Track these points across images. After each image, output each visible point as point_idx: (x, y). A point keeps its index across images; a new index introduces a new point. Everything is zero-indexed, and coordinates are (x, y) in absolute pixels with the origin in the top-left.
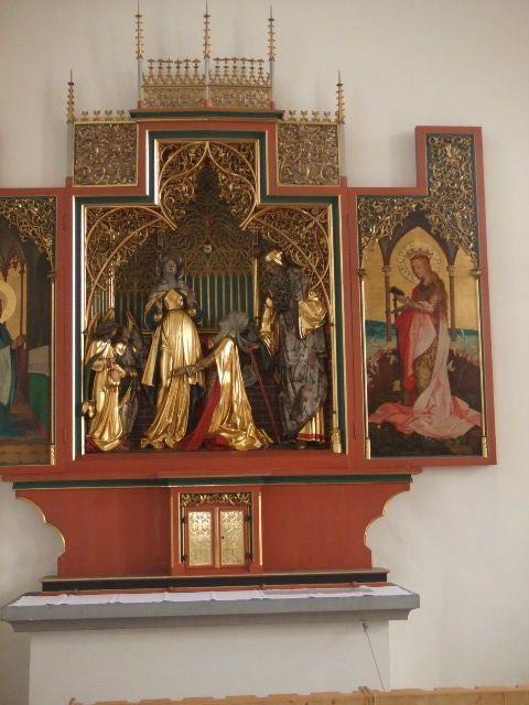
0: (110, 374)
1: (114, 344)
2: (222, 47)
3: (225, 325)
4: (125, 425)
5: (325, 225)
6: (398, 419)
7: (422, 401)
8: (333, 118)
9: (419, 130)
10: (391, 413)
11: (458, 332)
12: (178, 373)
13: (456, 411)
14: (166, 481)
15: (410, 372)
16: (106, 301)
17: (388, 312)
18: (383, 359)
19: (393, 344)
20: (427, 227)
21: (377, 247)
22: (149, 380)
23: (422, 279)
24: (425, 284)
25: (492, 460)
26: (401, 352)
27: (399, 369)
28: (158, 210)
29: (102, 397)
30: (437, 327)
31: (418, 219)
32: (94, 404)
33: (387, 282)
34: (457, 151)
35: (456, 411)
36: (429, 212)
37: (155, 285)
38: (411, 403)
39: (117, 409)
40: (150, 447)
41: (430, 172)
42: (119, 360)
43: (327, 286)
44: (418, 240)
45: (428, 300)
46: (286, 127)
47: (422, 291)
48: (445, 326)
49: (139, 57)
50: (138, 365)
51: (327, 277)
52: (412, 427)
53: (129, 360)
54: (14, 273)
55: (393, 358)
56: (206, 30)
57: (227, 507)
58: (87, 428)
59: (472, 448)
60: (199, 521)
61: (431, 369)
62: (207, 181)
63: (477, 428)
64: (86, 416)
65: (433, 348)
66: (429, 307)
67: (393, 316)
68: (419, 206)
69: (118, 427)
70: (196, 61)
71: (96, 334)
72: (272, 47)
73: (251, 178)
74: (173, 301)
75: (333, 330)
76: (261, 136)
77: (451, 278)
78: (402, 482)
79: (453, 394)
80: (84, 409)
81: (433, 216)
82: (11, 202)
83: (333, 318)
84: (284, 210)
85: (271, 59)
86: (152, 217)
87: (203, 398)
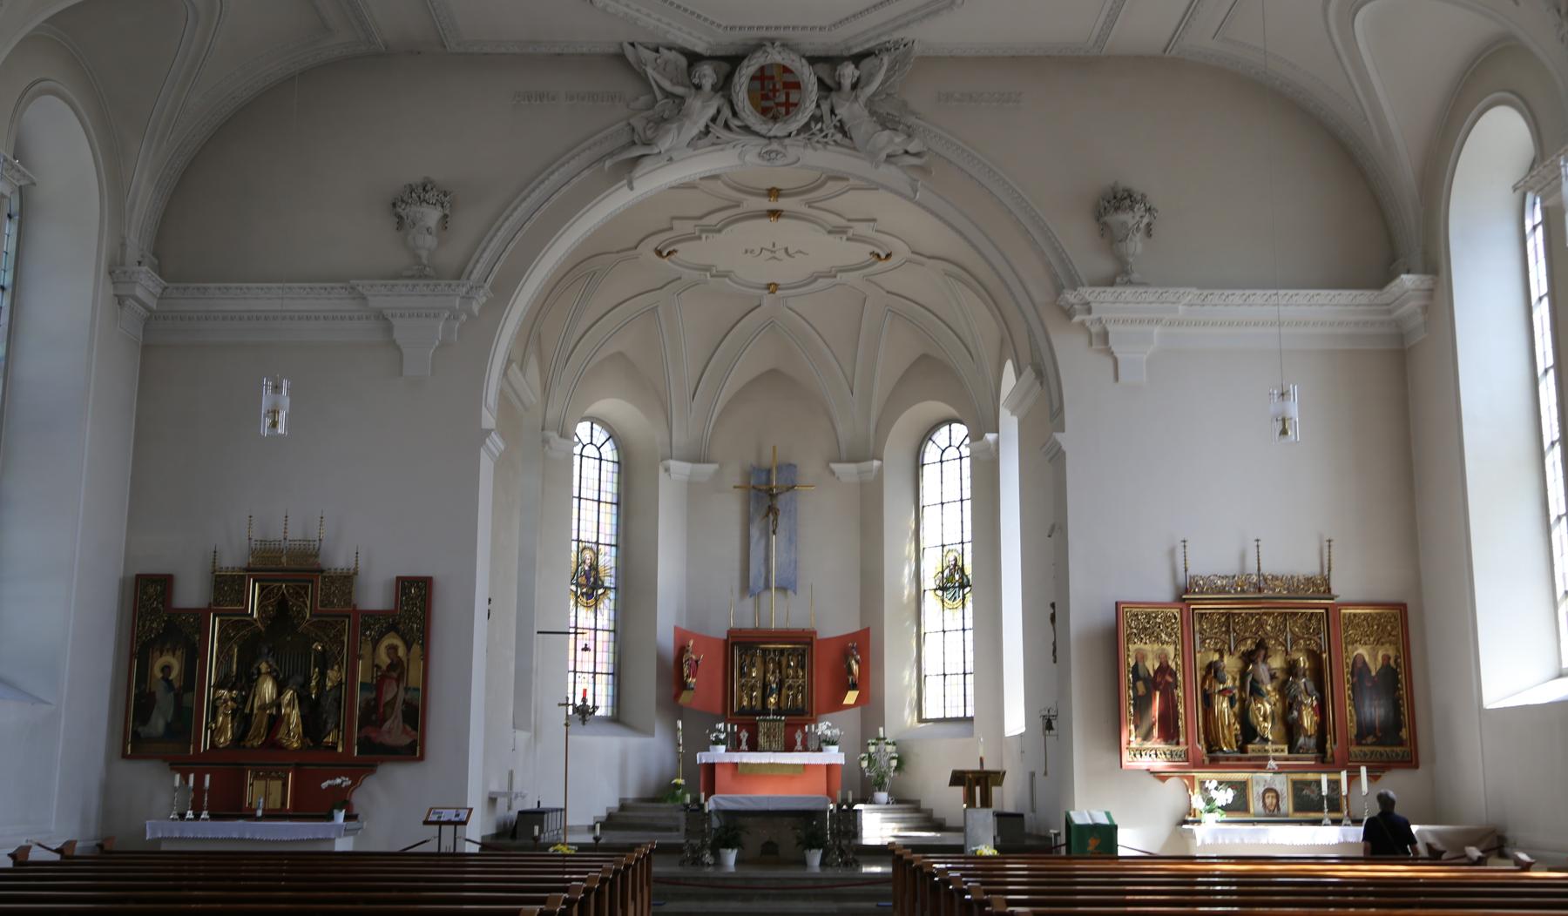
0: (225, 708)
1: (230, 690)
2: (296, 534)
4: (233, 734)
6: (373, 735)
7: (387, 725)
8: (352, 571)
11: (409, 689)
12: (263, 707)
14: (243, 764)
15: (382, 710)
16: (231, 667)
17: (372, 678)
19: (373, 695)
20: (397, 631)
21: (370, 643)
22: (247, 711)
23: (392, 660)
24: (395, 662)
25: (422, 758)
28: (255, 620)
30: (398, 687)
31: (393, 628)
32: (216, 723)
33: (373, 661)
35: (405, 731)
36: (398, 623)
38: (381, 726)
39: (230, 726)
40: (244, 746)
42: (233, 699)
43: (343, 663)
44: (392, 639)
45: (394, 671)
46: (325, 577)
47: (391, 667)
49: (250, 539)
50: (245, 700)
51: (343, 657)
54: (179, 653)
55: (373, 703)
56: (286, 524)
57: (273, 778)
59: (412, 752)
60: (259, 785)
61: (393, 709)
62: (282, 604)
63: (415, 741)
65: (395, 697)
66: (395, 675)
67: (375, 680)
68: (393, 621)
71: (219, 686)
73: (306, 605)
74: (264, 667)
75: (343, 686)
76: (312, 582)
77: (408, 660)
79: (404, 721)
80: (209, 726)
81: (401, 626)
82: (179, 616)
83: (344, 680)
84: (323, 621)
85: (320, 540)
86: (253, 624)
87: (276, 721)
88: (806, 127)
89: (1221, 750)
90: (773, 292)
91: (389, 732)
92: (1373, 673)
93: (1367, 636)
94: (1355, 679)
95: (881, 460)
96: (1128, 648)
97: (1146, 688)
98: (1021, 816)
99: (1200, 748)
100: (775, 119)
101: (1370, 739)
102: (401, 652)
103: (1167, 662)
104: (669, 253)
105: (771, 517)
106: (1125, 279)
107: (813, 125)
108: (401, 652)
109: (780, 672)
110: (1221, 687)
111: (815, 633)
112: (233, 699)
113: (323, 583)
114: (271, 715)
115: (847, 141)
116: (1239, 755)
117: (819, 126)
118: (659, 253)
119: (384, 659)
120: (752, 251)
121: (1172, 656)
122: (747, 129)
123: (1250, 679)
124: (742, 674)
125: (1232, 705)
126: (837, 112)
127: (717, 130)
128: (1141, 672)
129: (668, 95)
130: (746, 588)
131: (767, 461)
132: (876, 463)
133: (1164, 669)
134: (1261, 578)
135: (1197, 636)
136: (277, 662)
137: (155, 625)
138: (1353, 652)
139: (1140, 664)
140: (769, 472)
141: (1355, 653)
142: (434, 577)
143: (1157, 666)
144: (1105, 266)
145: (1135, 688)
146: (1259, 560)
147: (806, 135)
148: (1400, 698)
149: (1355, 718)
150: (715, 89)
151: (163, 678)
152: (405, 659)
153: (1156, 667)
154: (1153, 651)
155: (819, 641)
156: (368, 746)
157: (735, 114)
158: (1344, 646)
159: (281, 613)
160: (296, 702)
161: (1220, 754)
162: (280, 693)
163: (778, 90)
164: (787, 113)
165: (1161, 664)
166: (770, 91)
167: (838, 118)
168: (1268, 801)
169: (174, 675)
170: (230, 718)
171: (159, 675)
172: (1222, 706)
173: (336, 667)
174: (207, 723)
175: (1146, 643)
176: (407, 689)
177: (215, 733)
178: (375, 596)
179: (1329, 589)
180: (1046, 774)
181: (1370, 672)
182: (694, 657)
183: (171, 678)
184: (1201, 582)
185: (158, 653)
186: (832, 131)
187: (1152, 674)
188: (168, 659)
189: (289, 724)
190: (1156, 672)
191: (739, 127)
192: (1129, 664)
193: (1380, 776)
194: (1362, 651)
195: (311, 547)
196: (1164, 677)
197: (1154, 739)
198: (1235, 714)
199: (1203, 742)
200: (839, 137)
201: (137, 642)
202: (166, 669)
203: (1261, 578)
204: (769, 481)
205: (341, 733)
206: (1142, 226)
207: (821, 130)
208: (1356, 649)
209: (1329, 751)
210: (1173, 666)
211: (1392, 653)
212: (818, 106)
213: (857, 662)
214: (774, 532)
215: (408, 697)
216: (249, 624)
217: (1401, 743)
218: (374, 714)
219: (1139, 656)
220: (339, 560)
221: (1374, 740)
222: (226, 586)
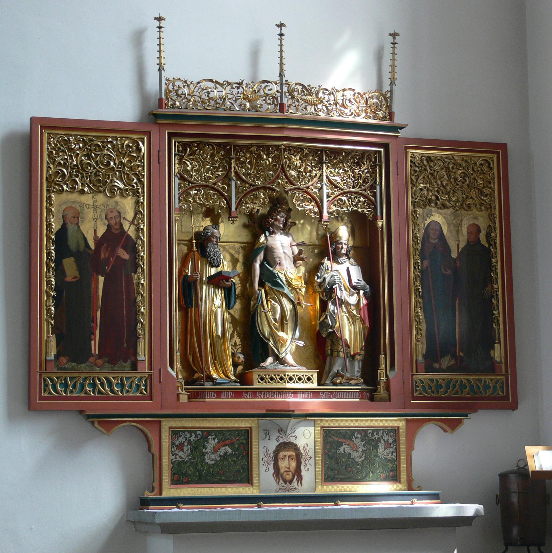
89: (210, 379)
92: (454, 255)
93: (447, 193)
94: (426, 262)
96: (49, 198)
97: (80, 269)
99: (174, 374)
101: (446, 362)
103: (121, 225)
110: (213, 271)
116: (238, 386)
121: (130, 215)
123: (260, 257)
128: (72, 242)
134: (285, 89)
135: (176, 182)
138: (424, 219)
139: (71, 228)
143: (101, 232)
145: (59, 271)
146: (281, 58)
148: (493, 295)
149: (424, 326)
153: (100, 234)
154: (95, 207)
161: (208, 385)
165: (109, 227)
168: (283, 464)
175: (82, 192)
179: (391, 115)
181: (450, 252)
184: (186, 91)
187: (92, 245)
190: (99, 242)
192: (49, 225)
193: (459, 422)
194: (437, 217)
196: (113, 252)
197: (91, 359)
198: (233, 320)
199: (178, 365)
203: (285, 89)
208: (430, 214)
209: (383, 379)
210: (131, 232)
211: (482, 223)
219: (70, 214)
221: (453, 362)
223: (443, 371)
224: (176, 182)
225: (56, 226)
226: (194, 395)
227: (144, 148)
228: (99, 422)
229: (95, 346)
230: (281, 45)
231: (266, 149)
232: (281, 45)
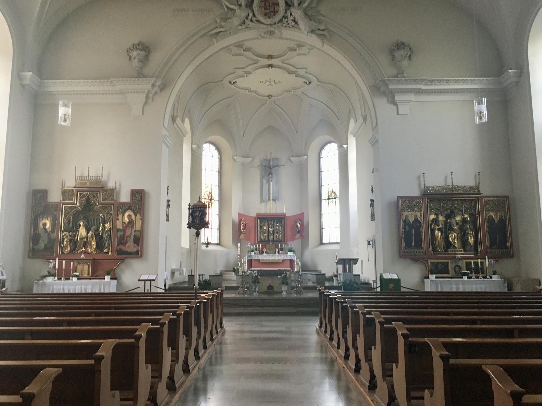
1: (69, 232)
2: (93, 174)
3: (92, 228)
5: (111, 209)
8: (114, 188)
9: (131, 190)
10: (122, 247)
11: (136, 231)
13: (134, 246)
15: (126, 238)
18: (121, 236)
19: (123, 233)
20: (131, 210)
22: (76, 240)
24: (130, 221)
25: (141, 256)
26: (124, 235)
27: (124, 237)
29: (65, 243)
30: (132, 230)
31: (130, 208)
32: (63, 244)
33: (123, 220)
34: (139, 194)
35: (134, 246)
37: (78, 221)
38: (125, 245)
41: (133, 198)
46: (104, 190)
47: (129, 223)
48: (133, 230)
52: (125, 250)
53: (73, 236)
54: (49, 218)
55: (122, 236)
58: (62, 249)
59: (138, 254)
61: (130, 238)
62: (88, 200)
64: (62, 246)
65: (131, 234)
66: (130, 226)
67: (123, 228)
69: (69, 249)
70: (87, 177)
72: (102, 174)
73: (97, 200)
74: (82, 223)
77: (135, 220)
78: (123, 260)
79: (134, 243)
80: (61, 245)
88: (281, 21)
90: (270, 98)
91: (129, 247)
95: (307, 156)
98: (359, 275)
100: (269, 17)
101: (495, 247)
102: (133, 217)
104: (234, 83)
105: (270, 176)
106: (402, 76)
107: (284, 19)
108: (133, 217)
109: (274, 228)
110: (438, 227)
111: (285, 214)
112: (70, 236)
113: (103, 192)
114: (84, 242)
115: (296, 25)
116: (445, 253)
117: (286, 20)
118: (230, 83)
119: (126, 220)
120: (263, 82)
121: (419, 216)
122: (258, 21)
123: (448, 224)
124: (261, 228)
125: (442, 234)
126: (293, 14)
127: (248, 22)
129: (229, 8)
130: (262, 201)
131: (269, 157)
132: (305, 157)
133: (416, 221)
135: (429, 208)
136: (87, 222)
137: (40, 208)
138: (488, 214)
140: (269, 160)
141: (489, 215)
142: (145, 189)
144: (394, 71)
145: (405, 228)
146: (452, 180)
147: (281, 24)
149: (489, 239)
150: (247, 6)
151: (43, 228)
152: (134, 220)
153: (413, 220)
155: (287, 217)
156: (120, 252)
157: (254, 16)
158: (484, 212)
159: (88, 205)
160: (94, 236)
162: (88, 233)
163: (271, 6)
164: (274, 15)
165: (415, 219)
166: (268, 6)
167: (293, 17)
169: (48, 226)
170: (69, 243)
171: (42, 227)
172: (438, 234)
173: (109, 223)
174: (60, 245)
176: (135, 231)
177: (63, 248)
178: (125, 197)
179: (479, 191)
180: (368, 261)
182: (245, 223)
183: (46, 228)
185: (41, 219)
186: (291, 21)
187: (411, 223)
188: (44, 221)
189: (91, 244)
191: (257, 21)
194: (491, 214)
195: (99, 179)
198: (442, 237)
200: (293, 23)
201: (33, 215)
202: (45, 225)
204: (269, 164)
205: (111, 248)
206: (408, 56)
207: (287, 22)
208: (490, 213)
210: (420, 220)
211: (503, 214)
212: (286, 12)
213: (300, 224)
214: (271, 181)
215: (136, 234)
216: (76, 207)
217: (507, 248)
218: (122, 241)
220: (111, 185)
222: (66, 194)
223: (495, 249)
224: (429, 208)
225: (404, 219)
226: (434, 255)
227: (421, 201)
228: (415, 261)
229: (413, 244)
230: (452, 177)
231: (449, 200)
232: (452, 177)
